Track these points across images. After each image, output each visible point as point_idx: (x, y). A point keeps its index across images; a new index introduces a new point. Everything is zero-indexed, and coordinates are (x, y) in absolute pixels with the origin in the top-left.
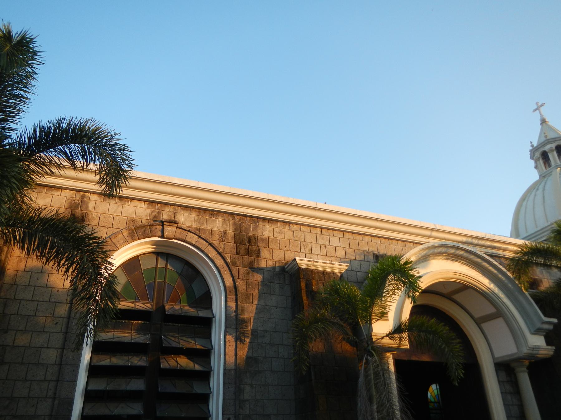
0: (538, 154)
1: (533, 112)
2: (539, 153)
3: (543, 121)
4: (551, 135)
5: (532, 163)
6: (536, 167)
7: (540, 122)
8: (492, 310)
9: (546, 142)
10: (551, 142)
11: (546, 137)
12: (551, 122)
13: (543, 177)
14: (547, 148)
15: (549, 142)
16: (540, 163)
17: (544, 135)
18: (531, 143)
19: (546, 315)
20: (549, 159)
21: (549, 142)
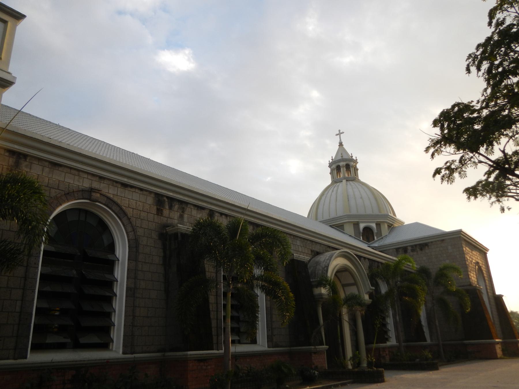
0: (334, 166)
1: (336, 135)
2: (335, 166)
3: (341, 144)
4: (345, 157)
5: (329, 170)
6: (330, 173)
7: (339, 144)
8: (352, 281)
9: (342, 160)
10: (344, 161)
11: (342, 157)
12: (345, 146)
13: (335, 181)
14: (341, 164)
15: (343, 160)
16: (335, 172)
17: (341, 155)
18: (332, 157)
19: (372, 286)
20: (340, 171)
21: (343, 160)
